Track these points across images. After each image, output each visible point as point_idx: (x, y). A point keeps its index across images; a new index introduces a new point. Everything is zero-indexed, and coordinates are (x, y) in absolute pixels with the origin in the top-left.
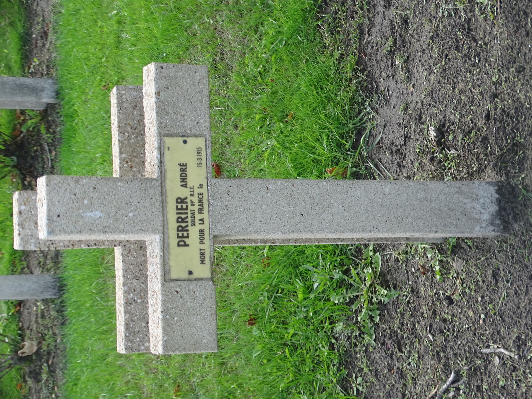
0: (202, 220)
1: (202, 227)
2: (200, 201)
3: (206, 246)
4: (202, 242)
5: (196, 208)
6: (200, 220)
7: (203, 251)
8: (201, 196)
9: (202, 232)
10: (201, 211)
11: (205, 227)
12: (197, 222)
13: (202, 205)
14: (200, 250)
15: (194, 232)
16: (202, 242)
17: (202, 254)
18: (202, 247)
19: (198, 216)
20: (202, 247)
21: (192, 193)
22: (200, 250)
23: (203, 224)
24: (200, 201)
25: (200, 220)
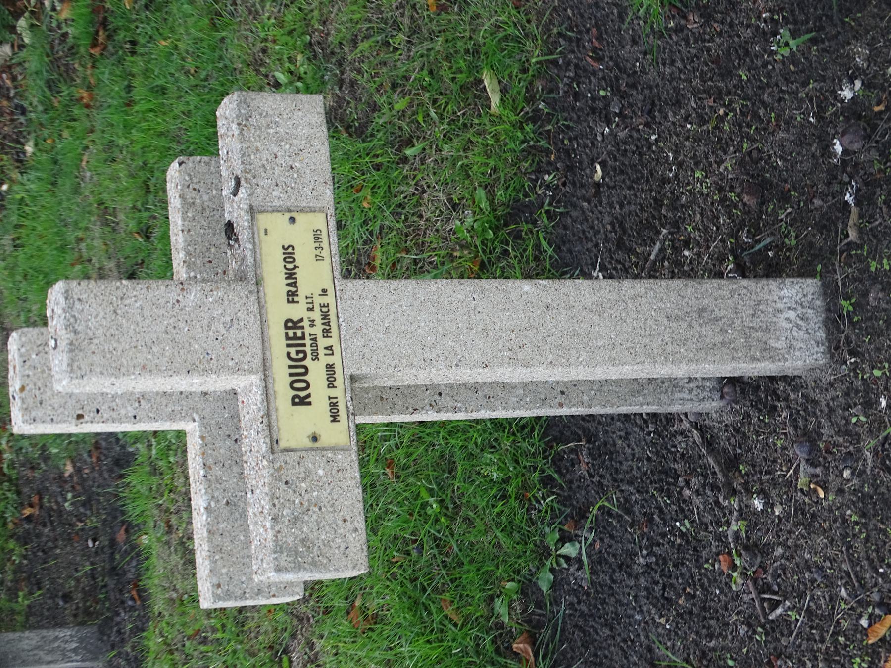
0: (330, 348)
1: (330, 360)
2: (325, 316)
6: (326, 348)
7: (334, 401)
8: (325, 309)
9: (330, 367)
10: (326, 333)
11: (335, 359)
12: (322, 352)
13: (328, 323)
14: (330, 398)
16: (331, 385)
17: (334, 405)
18: (332, 393)
19: (322, 343)
20: (332, 393)
22: (330, 398)
23: (332, 354)
24: (325, 316)
25: (326, 348)
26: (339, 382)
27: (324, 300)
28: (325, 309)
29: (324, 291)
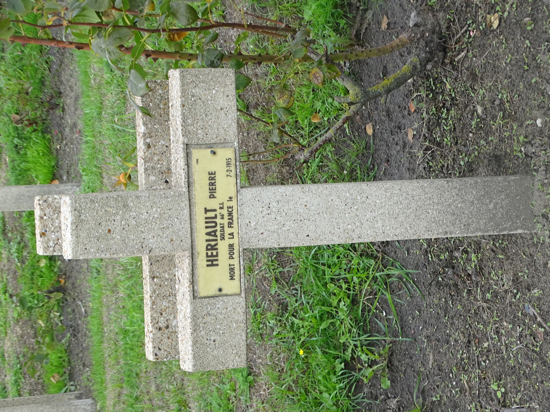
0: (232, 234)
1: (231, 241)
2: (230, 214)
3: (235, 262)
4: (231, 258)
5: (226, 221)
6: (229, 234)
7: (232, 267)
8: (230, 210)
9: (231, 246)
10: (230, 225)
11: (235, 241)
12: (227, 236)
13: (231, 219)
14: (230, 265)
15: (223, 247)
16: (231, 258)
17: (232, 270)
18: (232, 262)
19: (228, 231)
20: (232, 262)
21: (222, 206)
22: (230, 265)
23: (233, 238)
24: (230, 214)
25: (229, 234)
26: (236, 256)
27: (230, 204)
28: (230, 210)
29: (231, 198)
